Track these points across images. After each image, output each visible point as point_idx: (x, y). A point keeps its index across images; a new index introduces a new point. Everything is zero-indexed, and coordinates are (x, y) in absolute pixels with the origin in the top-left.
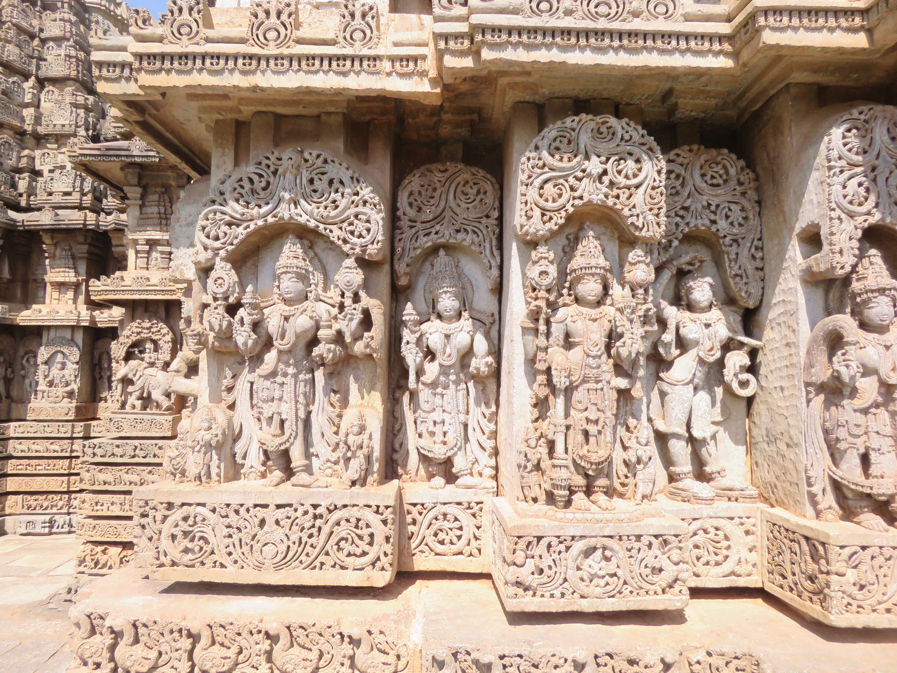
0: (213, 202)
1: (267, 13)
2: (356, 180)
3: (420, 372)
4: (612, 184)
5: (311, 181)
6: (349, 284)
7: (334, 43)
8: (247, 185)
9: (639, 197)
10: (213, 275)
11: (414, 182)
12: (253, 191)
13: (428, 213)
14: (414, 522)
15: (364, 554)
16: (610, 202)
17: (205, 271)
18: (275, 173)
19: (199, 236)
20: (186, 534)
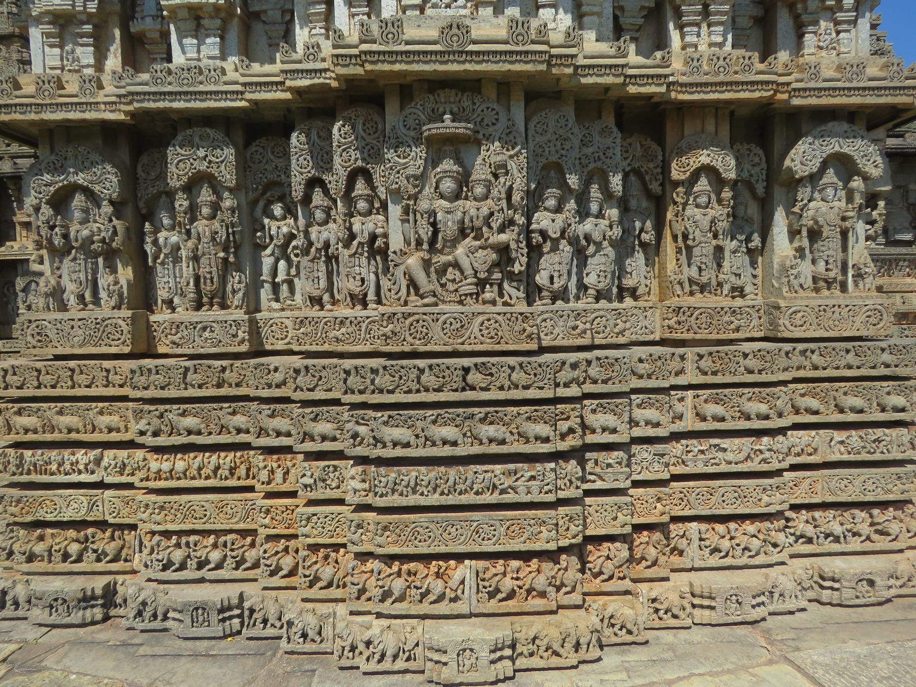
0: (37, 175)
1: (44, 82)
2: (103, 162)
3: (156, 258)
4: (210, 162)
5: (83, 162)
6: (106, 213)
7: (76, 96)
8: (52, 166)
9: (222, 168)
10: (41, 211)
11: (144, 159)
12: (56, 169)
13: (153, 175)
14: (155, 331)
15: (119, 339)
16: (209, 170)
17: (37, 209)
18: (65, 159)
19: (33, 192)
20: (38, 334)
